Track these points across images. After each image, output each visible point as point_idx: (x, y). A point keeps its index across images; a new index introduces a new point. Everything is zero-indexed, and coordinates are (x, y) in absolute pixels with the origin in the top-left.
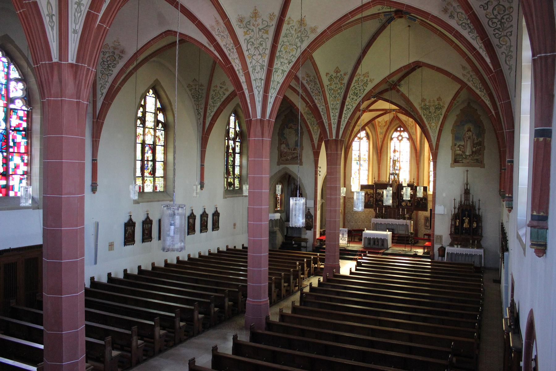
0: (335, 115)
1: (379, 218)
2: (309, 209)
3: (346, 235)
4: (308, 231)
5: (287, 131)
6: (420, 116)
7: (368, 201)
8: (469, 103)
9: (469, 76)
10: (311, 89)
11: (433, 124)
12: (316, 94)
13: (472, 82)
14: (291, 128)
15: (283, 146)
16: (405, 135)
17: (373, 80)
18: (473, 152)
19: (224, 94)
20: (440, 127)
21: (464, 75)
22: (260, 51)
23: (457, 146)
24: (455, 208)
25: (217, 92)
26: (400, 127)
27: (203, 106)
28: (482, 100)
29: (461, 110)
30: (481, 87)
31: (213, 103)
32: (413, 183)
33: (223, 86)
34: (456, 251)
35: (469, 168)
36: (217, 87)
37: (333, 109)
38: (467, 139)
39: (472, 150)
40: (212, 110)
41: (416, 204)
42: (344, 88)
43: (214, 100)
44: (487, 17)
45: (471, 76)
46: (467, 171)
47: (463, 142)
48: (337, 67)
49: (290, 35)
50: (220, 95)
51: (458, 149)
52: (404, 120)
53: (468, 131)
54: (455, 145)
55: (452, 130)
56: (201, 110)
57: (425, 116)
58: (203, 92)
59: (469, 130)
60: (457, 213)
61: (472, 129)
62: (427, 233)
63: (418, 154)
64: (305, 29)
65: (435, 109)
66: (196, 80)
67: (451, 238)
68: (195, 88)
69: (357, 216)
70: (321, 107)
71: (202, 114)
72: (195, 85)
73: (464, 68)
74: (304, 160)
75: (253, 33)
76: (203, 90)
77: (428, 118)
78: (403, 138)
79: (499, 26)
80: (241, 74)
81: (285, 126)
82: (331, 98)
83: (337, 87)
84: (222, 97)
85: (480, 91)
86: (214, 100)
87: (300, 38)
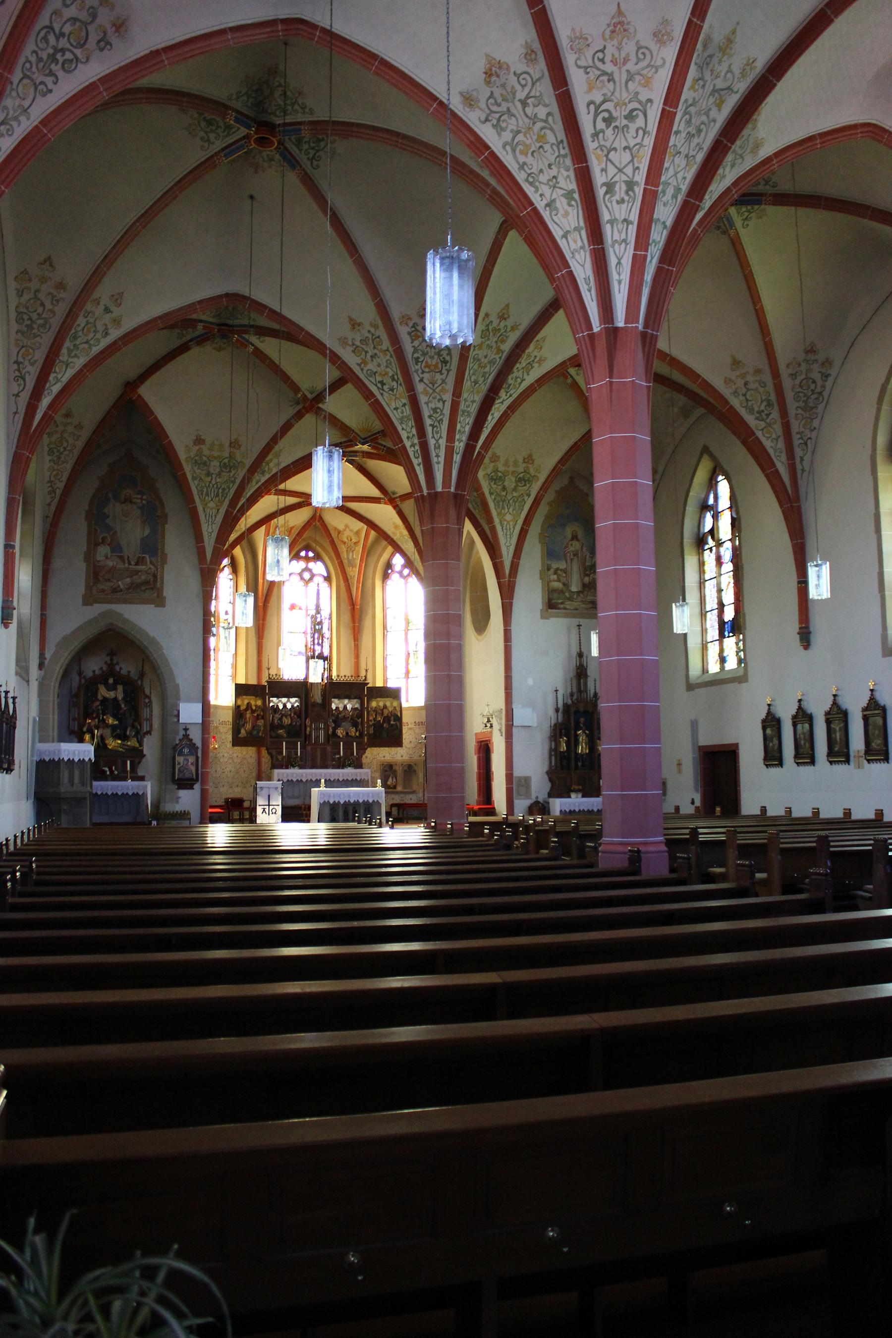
0: (462, 430)
1: (294, 767)
2: (186, 729)
3: (277, 800)
4: (183, 793)
5: (114, 509)
6: (483, 494)
7: (253, 727)
8: (572, 479)
9: (740, 382)
10: (416, 350)
11: (508, 517)
12: (427, 366)
13: (743, 398)
14: (128, 500)
15: (103, 551)
16: (318, 568)
17: (545, 359)
18: (584, 585)
19: (107, 334)
20: (524, 524)
21: (730, 380)
23: (552, 571)
24: (557, 710)
25: (92, 320)
26: (307, 548)
27: (40, 356)
28: (757, 438)
29: (556, 492)
30: (762, 408)
31: (70, 351)
32: (365, 679)
33: (113, 308)
34: (579, 805)
35: (582, 621)
36: (98, 304)
37: (464, 412)
38: (572, 557)
39: (582, 580)
40: (60, 376)
41: (371, 731)
42: (499, 362)
43: (75, 345)
45: (746, 384)
46: (579, 626)
47: (564, 563)
48: (508, 306)
50: (96, 332)
51: (555, 577)
52: (335, 529)
53: (572, 539)
54: (549, 569)
55: (540, 534)
56: (29, 368)
57: (493, 497)
58: (56, 309)
59: (574, 537)
60: (562, 724)
61: (579, 537)
62: (395, 802)
63: (357, 612)
65: (517, 482)
66: (51, 265)
67: (550, 780)
68: (37, 291)
69: (219, 769)
70: (432, 405)
71: (31, 381)
72: (43, 280)
73: (736, 363)
74: (169, 591)
76: (58, 301)
77: (498, 502)
78: (313, 576)
80: (617, 197)
81: (110, 495)
82: (469, 382)
83: (489, 356)
84: (98, 341)
85: (757, 419)
86: (75, 345)
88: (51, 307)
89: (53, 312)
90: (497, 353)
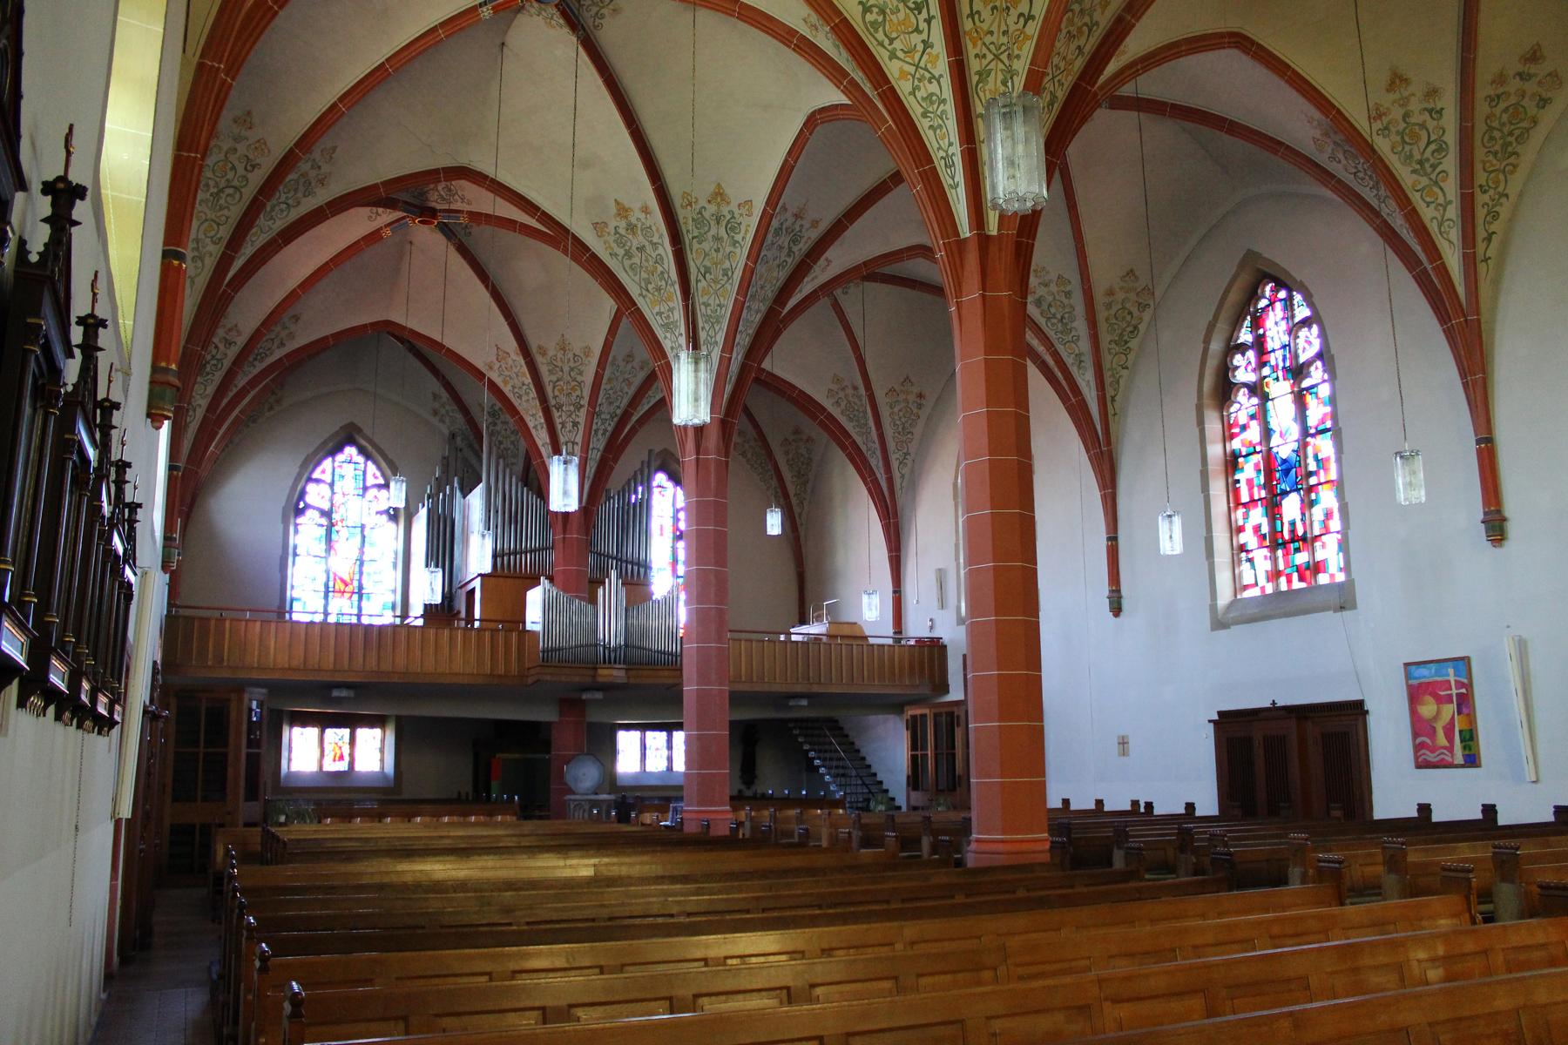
88: (244, 173)
89: (245, 178)
90: (789, 255)
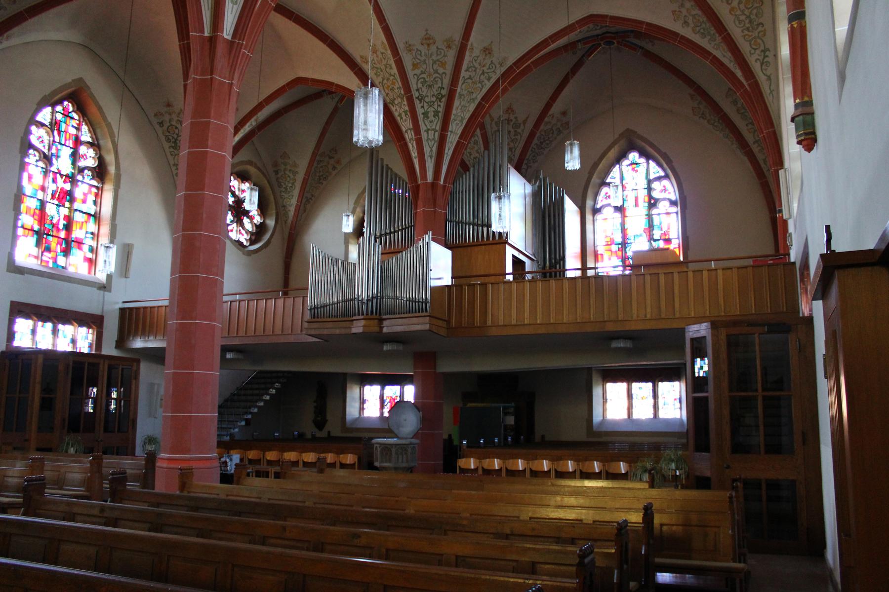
22: (434, 90)
44: (732, 14)
49: (473, 69)
64: (492, 61)
75: (425, 65)
79: (748, 25)
87: (486, 75)
